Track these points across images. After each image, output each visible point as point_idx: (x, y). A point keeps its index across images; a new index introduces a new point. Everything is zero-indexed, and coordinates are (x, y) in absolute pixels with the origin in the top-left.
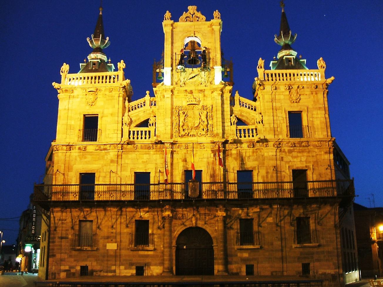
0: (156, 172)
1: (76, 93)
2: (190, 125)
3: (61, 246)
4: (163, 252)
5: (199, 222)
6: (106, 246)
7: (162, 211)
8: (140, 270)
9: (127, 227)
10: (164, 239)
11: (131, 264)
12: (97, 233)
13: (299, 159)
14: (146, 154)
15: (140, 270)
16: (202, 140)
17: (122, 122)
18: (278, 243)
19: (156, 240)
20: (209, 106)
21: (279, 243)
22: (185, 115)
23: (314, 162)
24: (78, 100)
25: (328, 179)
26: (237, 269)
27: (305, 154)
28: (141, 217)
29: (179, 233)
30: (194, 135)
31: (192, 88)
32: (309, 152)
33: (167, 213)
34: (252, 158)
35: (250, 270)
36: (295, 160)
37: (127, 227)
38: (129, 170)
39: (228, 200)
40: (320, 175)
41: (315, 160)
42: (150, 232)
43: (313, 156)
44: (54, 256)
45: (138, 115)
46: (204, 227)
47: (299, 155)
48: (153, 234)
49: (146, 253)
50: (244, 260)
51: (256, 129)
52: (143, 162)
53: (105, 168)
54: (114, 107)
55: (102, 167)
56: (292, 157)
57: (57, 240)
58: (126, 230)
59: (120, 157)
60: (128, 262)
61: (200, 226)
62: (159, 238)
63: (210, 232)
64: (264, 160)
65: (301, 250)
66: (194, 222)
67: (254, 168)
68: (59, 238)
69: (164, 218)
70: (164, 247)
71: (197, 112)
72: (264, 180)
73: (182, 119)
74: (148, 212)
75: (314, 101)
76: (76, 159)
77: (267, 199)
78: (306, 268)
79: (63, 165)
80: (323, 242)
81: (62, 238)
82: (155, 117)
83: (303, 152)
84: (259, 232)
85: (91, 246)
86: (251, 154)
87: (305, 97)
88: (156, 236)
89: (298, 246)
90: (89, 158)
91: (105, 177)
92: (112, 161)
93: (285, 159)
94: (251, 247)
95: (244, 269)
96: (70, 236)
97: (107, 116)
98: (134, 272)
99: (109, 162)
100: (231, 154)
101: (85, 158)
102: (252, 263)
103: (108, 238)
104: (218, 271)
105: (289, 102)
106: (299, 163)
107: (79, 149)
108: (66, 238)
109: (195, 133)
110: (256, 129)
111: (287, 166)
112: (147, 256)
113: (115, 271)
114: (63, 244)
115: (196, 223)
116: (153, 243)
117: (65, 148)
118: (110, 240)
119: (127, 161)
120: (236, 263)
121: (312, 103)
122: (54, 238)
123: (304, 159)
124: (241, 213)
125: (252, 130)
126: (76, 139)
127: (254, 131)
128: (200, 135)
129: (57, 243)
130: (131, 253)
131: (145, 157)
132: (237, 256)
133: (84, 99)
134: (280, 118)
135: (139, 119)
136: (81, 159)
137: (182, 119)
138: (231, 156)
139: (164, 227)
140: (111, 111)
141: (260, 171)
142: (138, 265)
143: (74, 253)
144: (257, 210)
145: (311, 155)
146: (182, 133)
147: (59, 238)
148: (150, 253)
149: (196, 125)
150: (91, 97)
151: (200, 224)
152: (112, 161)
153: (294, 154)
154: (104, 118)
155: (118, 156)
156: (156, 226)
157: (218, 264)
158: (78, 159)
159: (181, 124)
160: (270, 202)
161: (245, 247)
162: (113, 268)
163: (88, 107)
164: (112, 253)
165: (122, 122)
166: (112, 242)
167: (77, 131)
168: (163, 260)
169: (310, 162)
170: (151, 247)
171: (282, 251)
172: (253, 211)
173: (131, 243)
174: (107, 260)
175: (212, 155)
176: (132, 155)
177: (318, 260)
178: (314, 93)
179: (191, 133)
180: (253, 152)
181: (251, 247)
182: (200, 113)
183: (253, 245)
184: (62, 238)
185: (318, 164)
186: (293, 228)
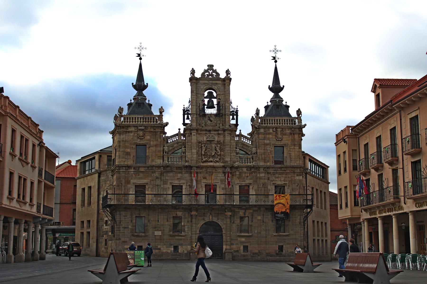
0: (186, 185)
1: (130, 129)
2: (209, 154)
3: (124, 233)
4: (191, 237)
5: (213, 218)
6: (154, 233)
7: (191, 212)
8: (176, 248)
9: (167, 221)
10: (191, 229)
11: (171, 245)
12: (148, 225)
13: (280, 179)
14: (180, 173)
15: (176, 248)
16: (217, 164)
17: (163, 150)
18: (263, 232)
19: (186, 229)
20: (222, 141)
21: (265, 232)
23: (289, 181)
24: (132, 134)
25: (297, 193)
26: (237, 248)
27: (284, 176)
28: (177, 214)
29: (201, 225)
30: (211, 162)
31: (211, 128)
32: (286, 174)
33: (193, 213)
34: (249, 177)
35: (246, 248)
36: (277, 179)
37: (167, 221)
38: (169, 184)
39: (234, 205)
40: (293, 189)
41: (290, 179)
42: (183, 224)
43: (289, 177)
44: (120, 239)
45: (173, 146)
46: (217, 222)
47: (280, 176)
48: (184, 226)
49: (180, 238)
50: (242, 242)
51: (253, 158)
52: (178, 179)
53: (152, 182)
54: (157, 140)
55: (151, 181)
56: (275, 177)
57: (121, 229)
58: (167, 223)
59: (162, 175)
60: (168, 243)
61: (215, 221)
62: (188, 228)
63: (221, 225)
64: (257, 179)
65: (278, 237)
66: (211, 218)
67: (251, 184)
68: (123, 228)
69: (192, 216)
70: (191, 234)
71: (214, 145)
72: (256, 192)
73: (204, 150)
74: (181, 211)
75: (292, 140)
76: (132, 176)
77: (258, 205)
78: (281, 248)
79: (124, 180)
80: (292, 232)
81: (125, 228)
82: (185, 147)
83: (282, 174)
84: (251, 225)
85: (144, 233)
86: (248, 175)
87: (286, 136)
88: (186, 227)
89: (276, 234)
90: (141, 175)
91: (153, 188)
92: (157, 178)
93: (270, 179)
94: (247, 234)
95: (242, 248)
96: (130, 227)
97: (153, 147)
98: (173, 249)
99: (155, 178)
100: (236, 175)
101: (139, 175)
102: (247, 244)
103: (155, 228)
104: (226, 249)
105: (275, 140)
106: (279, 181)
107: (134, 168)
108: (128, 228)
109: (212, 160)
110: (253, 158)
111: (272, 183)
112: (181, 239)
113: (160, 249)
114: (125, 231)
115: (212, 219)
116: (184, 231)
117: (124, 168)
118: (156, 229)
119: (167, 178)
120: (237, 244)
121: (291, 141)
122: (119, 228)
123: (282, 179)
124: (241, 213)
125: (250, 159)
126: (132, 162)
127: (251, 159)
129: (121, 231)
130: (171, 238)
131: (179, 175)
132: (237, 240)
133: (136, 134)
134: (269, 151)
135: (174, 149)
136: (136, 176)
137: (204, 150)
138: (235, 176)
139: (191, 222)
140: (155, 143)
141: (254, 186)
142: (175, 245)
143: (133, 238)
144: (251, 211)
145: (287, 176)
146: (204, 160)
147: (123, 228)
148: (182, 237)
149: (213, 154)
150: (141, 133)
151: (215, 220)
152: (157, 178)
153: (277, 175)
154: (151, 148)
155: (161, 174)
156: (186, 220)
157: (226, 245)
158: (134, 176)
159: (203, 153)
160: (260, 206)
161: (243, 234)
162: (159, 247)
163: (139, 140)
164: (158, 238)
165: (163, 150)
166: (158, 230)
167: (132, 156)
168: (192, 242)
169: (286, 181)
170: (183, 234)
171: (266, 237)
172: (249, 212)
173: (170, 231)
174: (155, 242)
175: (223, 175)
176: (171, 174)
177: (289, 244)
178: (292, 134)
179: (210, 160)
180: (250, 174)
181: (247, 234)
183: (249, 233)
184: (125, 228)
185: (292, 183)
186: (274, 224)
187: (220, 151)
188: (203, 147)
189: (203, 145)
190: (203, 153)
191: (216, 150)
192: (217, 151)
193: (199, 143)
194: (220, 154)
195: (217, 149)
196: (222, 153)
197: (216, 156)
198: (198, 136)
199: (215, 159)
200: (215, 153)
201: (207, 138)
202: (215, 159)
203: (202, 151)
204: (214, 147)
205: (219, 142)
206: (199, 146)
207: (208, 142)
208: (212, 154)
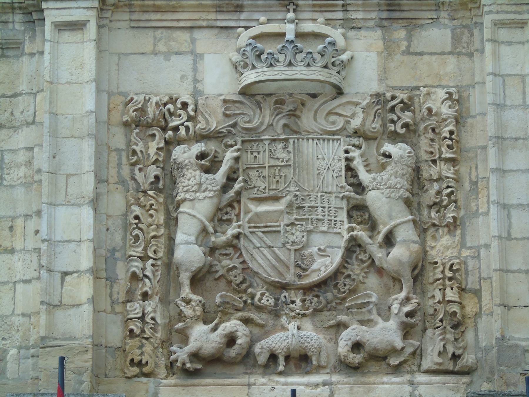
20: (438, 102)
22: (220, 175)
128: (356, 358)
137: (196, 209)
146: (203, 337)
149: (323, 266)
179: (279, 340)
182: (358, 164)
187: (422, 229)
188: (192, 177)
189: (180, 153)
190: (189, 252)
191: (358, 211)
192: (372, 226)
193: (138, 123)
194: (419, 270)
195: (375, 199)
196: (443, 248)
197: (372, 287)
198: (124, 39)
199: (353, 332)
200: (354, 246)
201: (238, 68)
202: (353, 332)
203: (172, 222)
204: (335, 183)
205: (396, 116)
206: (136, 160)
207: (260, 118)
208: (302, 268)
